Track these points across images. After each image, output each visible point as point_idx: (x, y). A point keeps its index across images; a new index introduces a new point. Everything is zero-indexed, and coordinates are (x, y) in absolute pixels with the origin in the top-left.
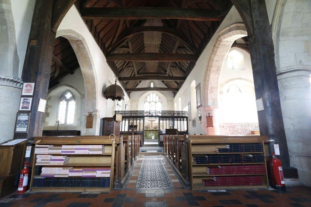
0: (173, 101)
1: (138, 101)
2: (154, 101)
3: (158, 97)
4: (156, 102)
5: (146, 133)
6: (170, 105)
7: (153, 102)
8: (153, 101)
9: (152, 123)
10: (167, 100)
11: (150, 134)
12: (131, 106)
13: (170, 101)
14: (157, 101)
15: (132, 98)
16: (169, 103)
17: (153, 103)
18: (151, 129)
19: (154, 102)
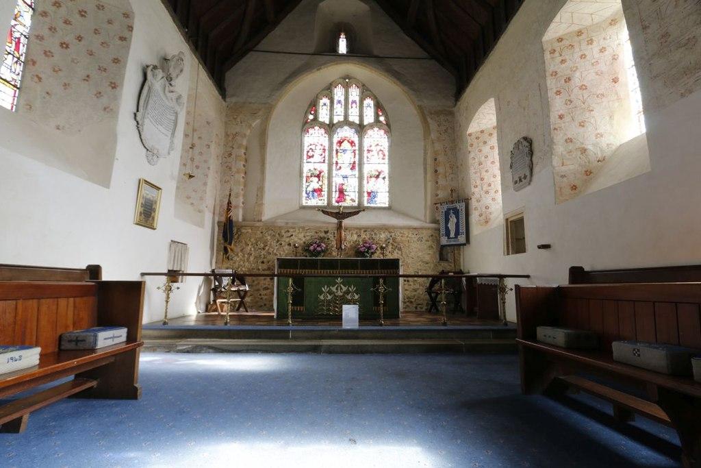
0: (452, 114)
1: (270, 109)
2: (351, 119)
3: (369, 102)
4: (361, 128)
5: (299, 281)
6: (433, 136)
7: (346, 128)
8: (346, 122)
9: (340, 226)
10: (421, 109)
11: (325, 289)
12: (227, 135)
13: (438, 113)
14: (369, 117)
15: (233, 96)
16: (433, 125)
17: (347, 132)
18: (335, 255)
19: (351, 124)
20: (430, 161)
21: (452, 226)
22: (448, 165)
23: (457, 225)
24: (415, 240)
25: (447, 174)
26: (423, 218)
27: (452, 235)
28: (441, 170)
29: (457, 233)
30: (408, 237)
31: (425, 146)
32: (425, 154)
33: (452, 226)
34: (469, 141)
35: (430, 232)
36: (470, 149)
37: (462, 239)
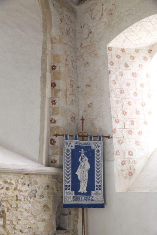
6: (55, 32)
20: (48, 67)
21: (82, 173)
22: (68, 81)
23: (91, 173)
24: (26, 194)
25: (68, 93)
26: (37, 157)
27: (83, 189)
28: (61, 84)
29: (91, 187)
30: (16, 189)
31: (45, 43)
32: (44, 52)
33: (82, 173)
34: (109, 57)
35: (46, 180)
36: (110, 67)
37: (97, 196)
